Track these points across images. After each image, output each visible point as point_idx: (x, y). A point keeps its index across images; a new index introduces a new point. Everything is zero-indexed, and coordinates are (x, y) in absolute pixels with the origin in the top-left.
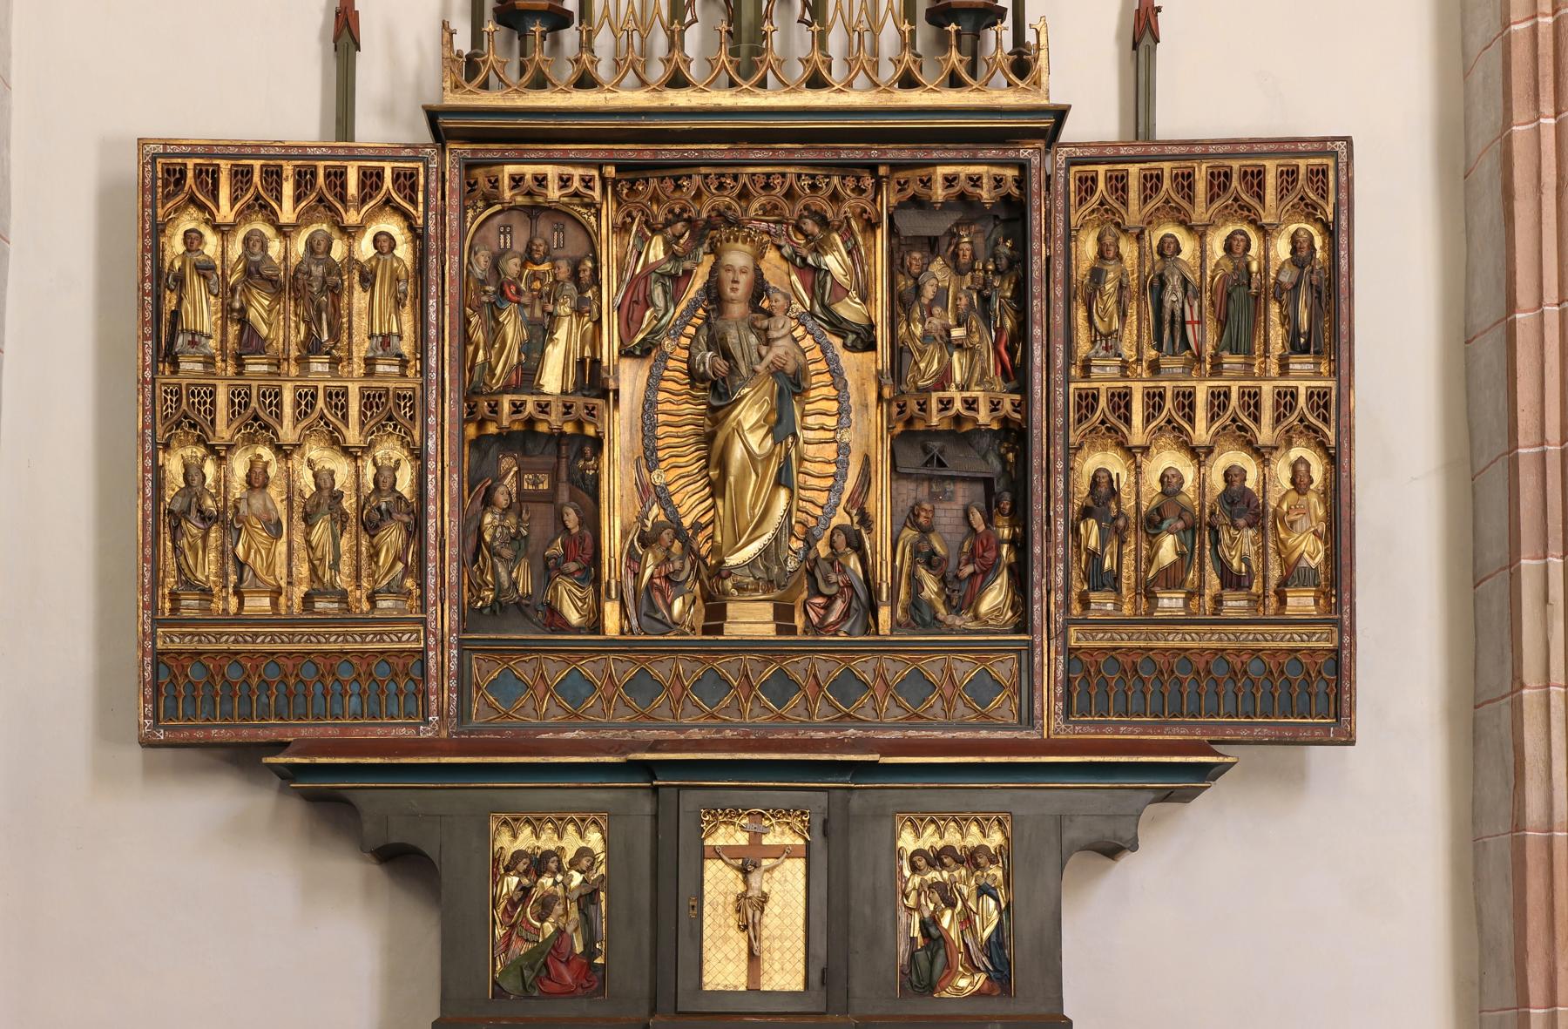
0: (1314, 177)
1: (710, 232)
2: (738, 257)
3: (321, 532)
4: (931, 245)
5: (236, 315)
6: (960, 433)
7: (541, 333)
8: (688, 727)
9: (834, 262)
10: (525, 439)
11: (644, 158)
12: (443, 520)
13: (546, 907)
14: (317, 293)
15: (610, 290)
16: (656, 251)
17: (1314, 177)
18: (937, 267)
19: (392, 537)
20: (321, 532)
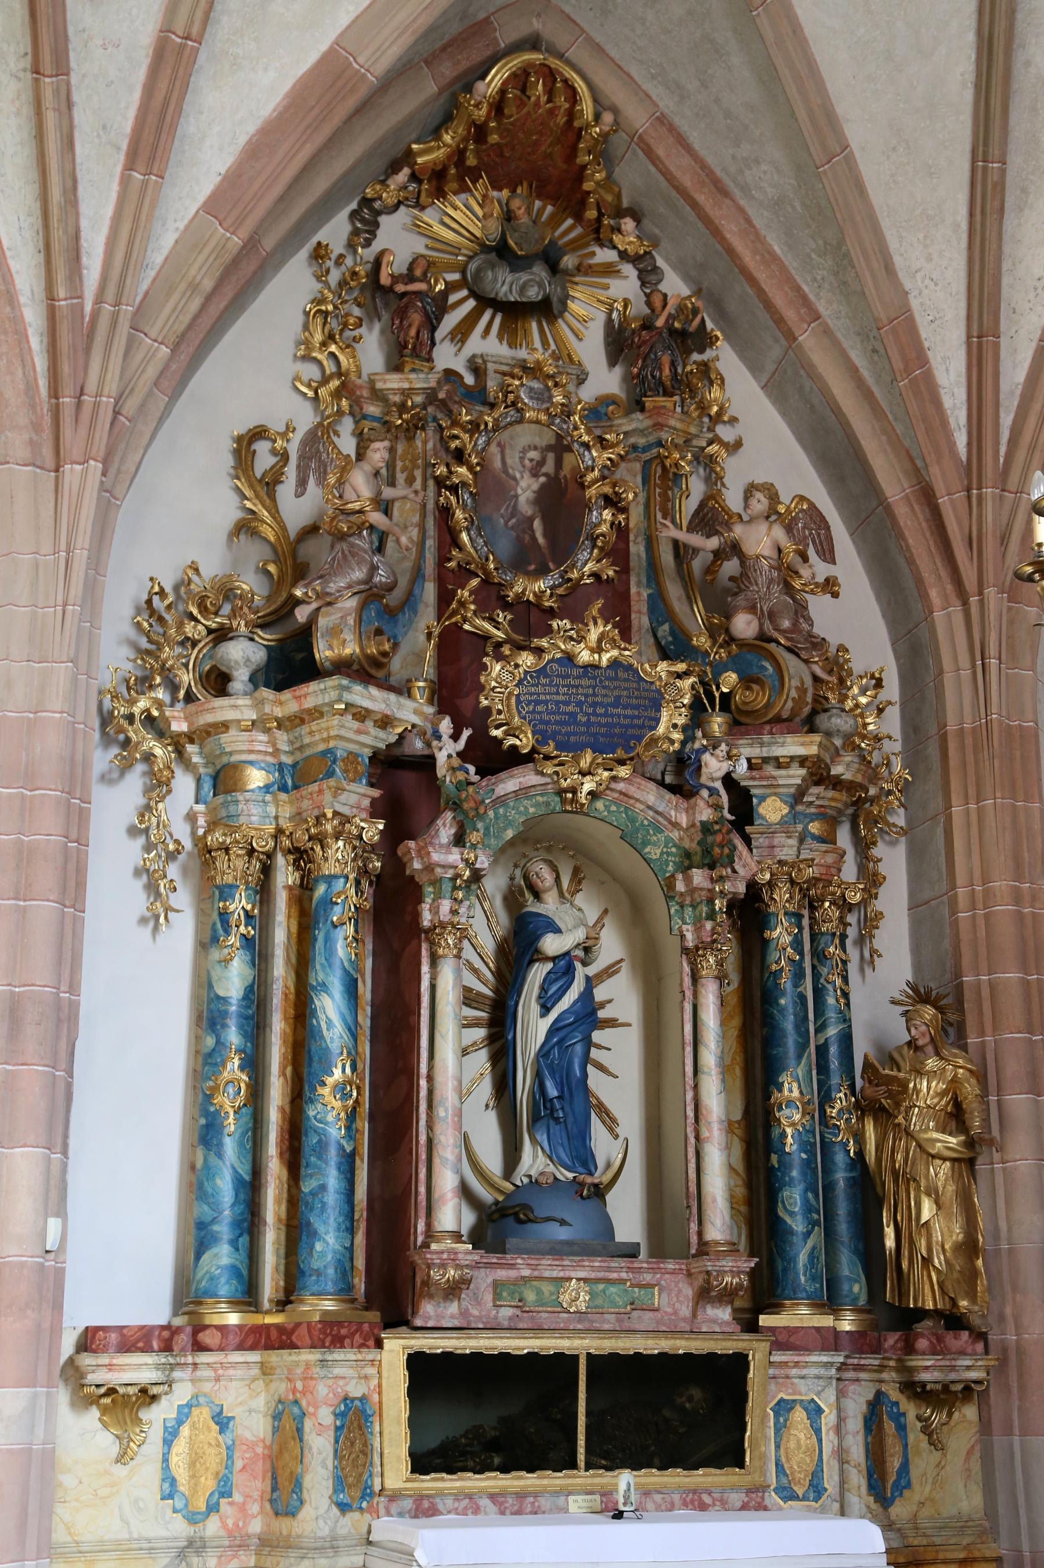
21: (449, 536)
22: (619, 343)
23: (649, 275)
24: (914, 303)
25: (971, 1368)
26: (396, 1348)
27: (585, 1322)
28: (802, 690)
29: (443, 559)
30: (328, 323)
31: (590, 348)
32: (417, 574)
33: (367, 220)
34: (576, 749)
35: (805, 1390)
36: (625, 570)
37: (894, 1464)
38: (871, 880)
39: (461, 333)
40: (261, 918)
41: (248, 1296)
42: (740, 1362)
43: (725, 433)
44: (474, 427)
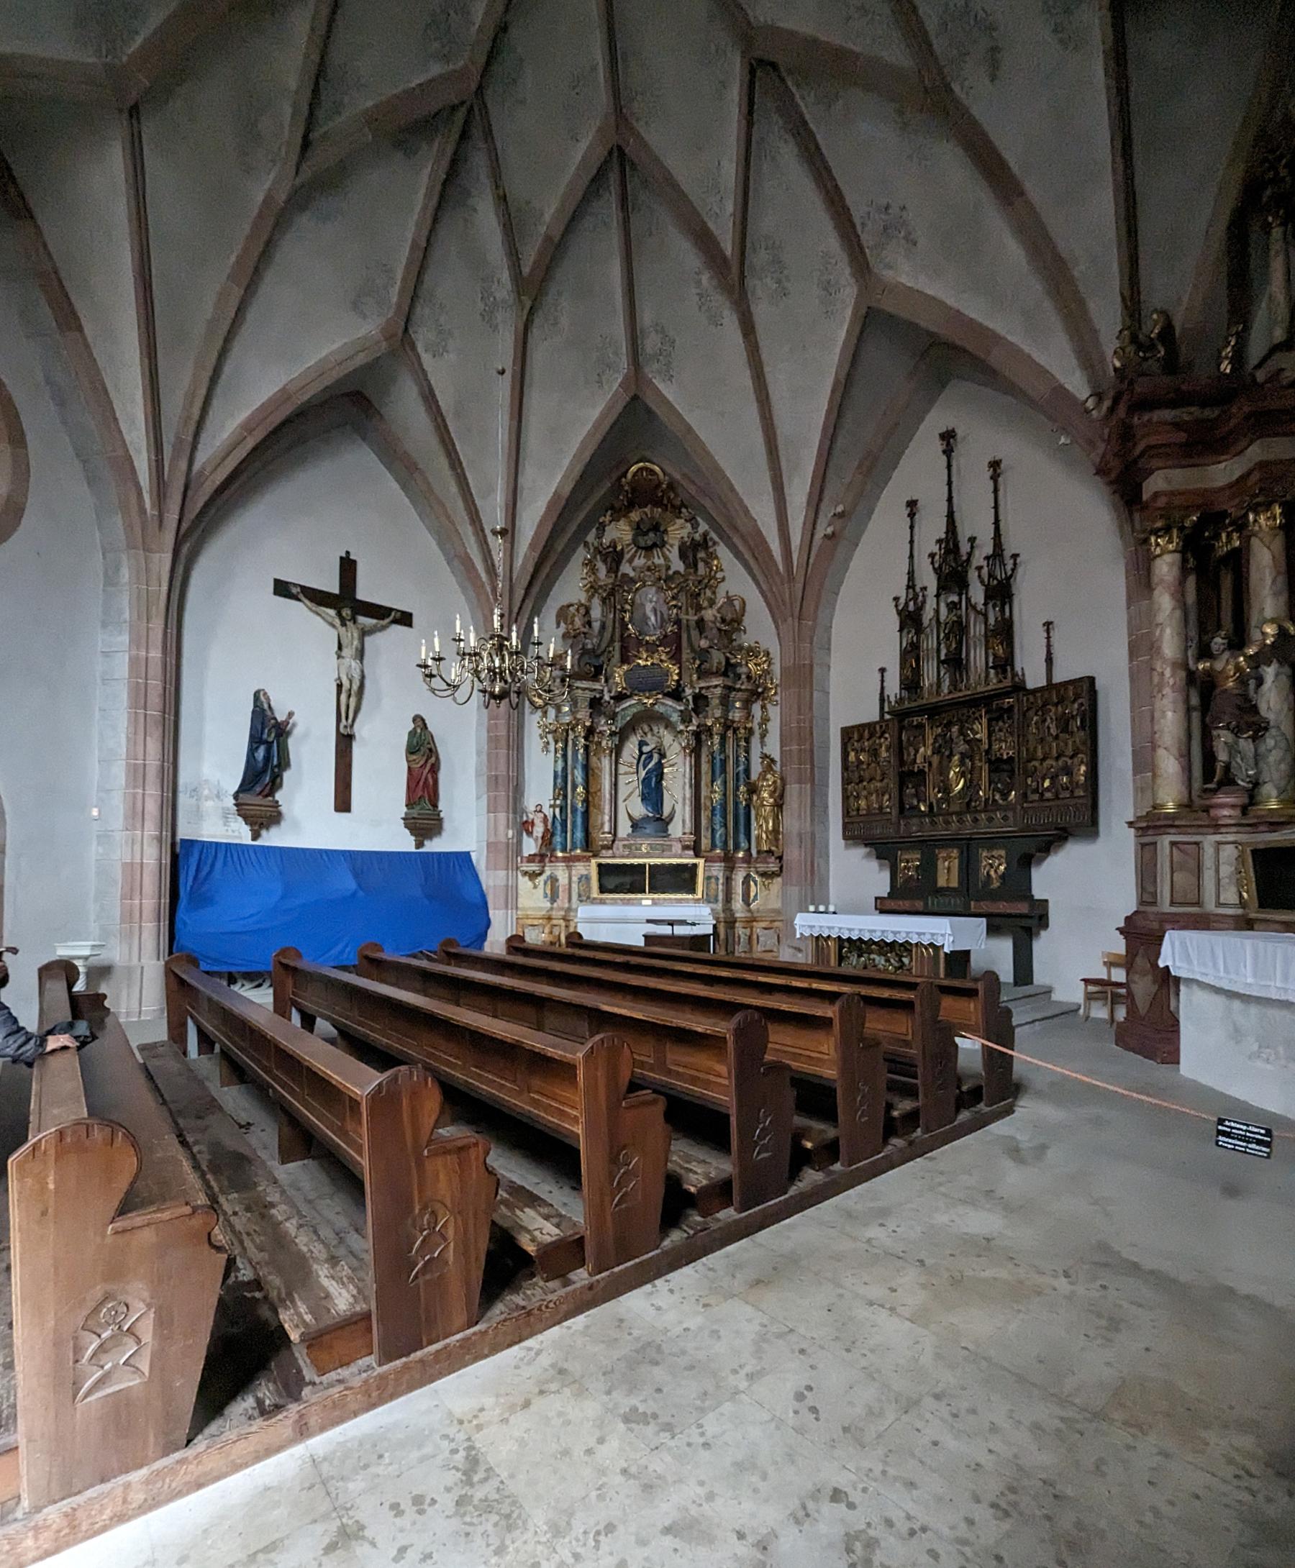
0: (1087, 687)
1: (949, 725)
2: (955, 729)
3: (874, 797)
4: (997, 719)
5: (857, 758)
6: (1000, 760)
7: (917, 751)
8: (941, 832)
9: (977, 726)
10: (911, 773)
11: (933, 711)
12: (895, 793)
13: (909, 869)
14: (874, 753)
15: (931, 741)
16: (939, 730)
17: (1087, 687)
18: (1001, 723)
19: (886, 797)
20: (874, 797)
21: (624, 626)
22: (683, 555)
23: (695, 526)
24: (759, 523)
25: (773, 866)
26: (594, 862)
27: (648, 855)
28: (719, 663)
29: (622, 635)
30: (589, 564)
31: (674, 554)
32: (612, 641)
33: (602, 528)
34: (644, 691)
35: (715, 873)
36: (680, 629)
37: (752, 894)
38: (765, 720)
39: (631, 561)
40: (565, 749)
41: (564, 850)
42: (695, 866)
43: (719, 575)
44: (629, 592)
